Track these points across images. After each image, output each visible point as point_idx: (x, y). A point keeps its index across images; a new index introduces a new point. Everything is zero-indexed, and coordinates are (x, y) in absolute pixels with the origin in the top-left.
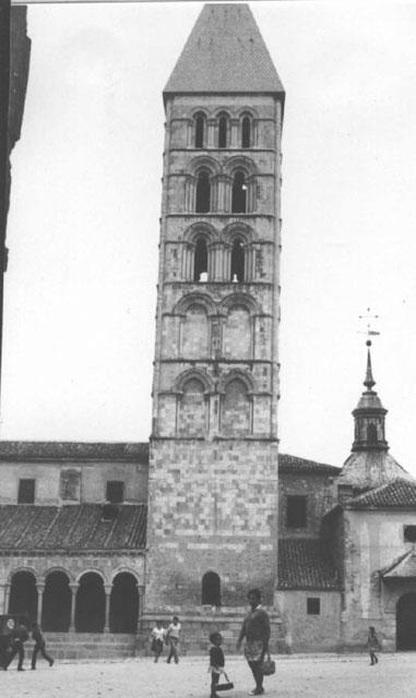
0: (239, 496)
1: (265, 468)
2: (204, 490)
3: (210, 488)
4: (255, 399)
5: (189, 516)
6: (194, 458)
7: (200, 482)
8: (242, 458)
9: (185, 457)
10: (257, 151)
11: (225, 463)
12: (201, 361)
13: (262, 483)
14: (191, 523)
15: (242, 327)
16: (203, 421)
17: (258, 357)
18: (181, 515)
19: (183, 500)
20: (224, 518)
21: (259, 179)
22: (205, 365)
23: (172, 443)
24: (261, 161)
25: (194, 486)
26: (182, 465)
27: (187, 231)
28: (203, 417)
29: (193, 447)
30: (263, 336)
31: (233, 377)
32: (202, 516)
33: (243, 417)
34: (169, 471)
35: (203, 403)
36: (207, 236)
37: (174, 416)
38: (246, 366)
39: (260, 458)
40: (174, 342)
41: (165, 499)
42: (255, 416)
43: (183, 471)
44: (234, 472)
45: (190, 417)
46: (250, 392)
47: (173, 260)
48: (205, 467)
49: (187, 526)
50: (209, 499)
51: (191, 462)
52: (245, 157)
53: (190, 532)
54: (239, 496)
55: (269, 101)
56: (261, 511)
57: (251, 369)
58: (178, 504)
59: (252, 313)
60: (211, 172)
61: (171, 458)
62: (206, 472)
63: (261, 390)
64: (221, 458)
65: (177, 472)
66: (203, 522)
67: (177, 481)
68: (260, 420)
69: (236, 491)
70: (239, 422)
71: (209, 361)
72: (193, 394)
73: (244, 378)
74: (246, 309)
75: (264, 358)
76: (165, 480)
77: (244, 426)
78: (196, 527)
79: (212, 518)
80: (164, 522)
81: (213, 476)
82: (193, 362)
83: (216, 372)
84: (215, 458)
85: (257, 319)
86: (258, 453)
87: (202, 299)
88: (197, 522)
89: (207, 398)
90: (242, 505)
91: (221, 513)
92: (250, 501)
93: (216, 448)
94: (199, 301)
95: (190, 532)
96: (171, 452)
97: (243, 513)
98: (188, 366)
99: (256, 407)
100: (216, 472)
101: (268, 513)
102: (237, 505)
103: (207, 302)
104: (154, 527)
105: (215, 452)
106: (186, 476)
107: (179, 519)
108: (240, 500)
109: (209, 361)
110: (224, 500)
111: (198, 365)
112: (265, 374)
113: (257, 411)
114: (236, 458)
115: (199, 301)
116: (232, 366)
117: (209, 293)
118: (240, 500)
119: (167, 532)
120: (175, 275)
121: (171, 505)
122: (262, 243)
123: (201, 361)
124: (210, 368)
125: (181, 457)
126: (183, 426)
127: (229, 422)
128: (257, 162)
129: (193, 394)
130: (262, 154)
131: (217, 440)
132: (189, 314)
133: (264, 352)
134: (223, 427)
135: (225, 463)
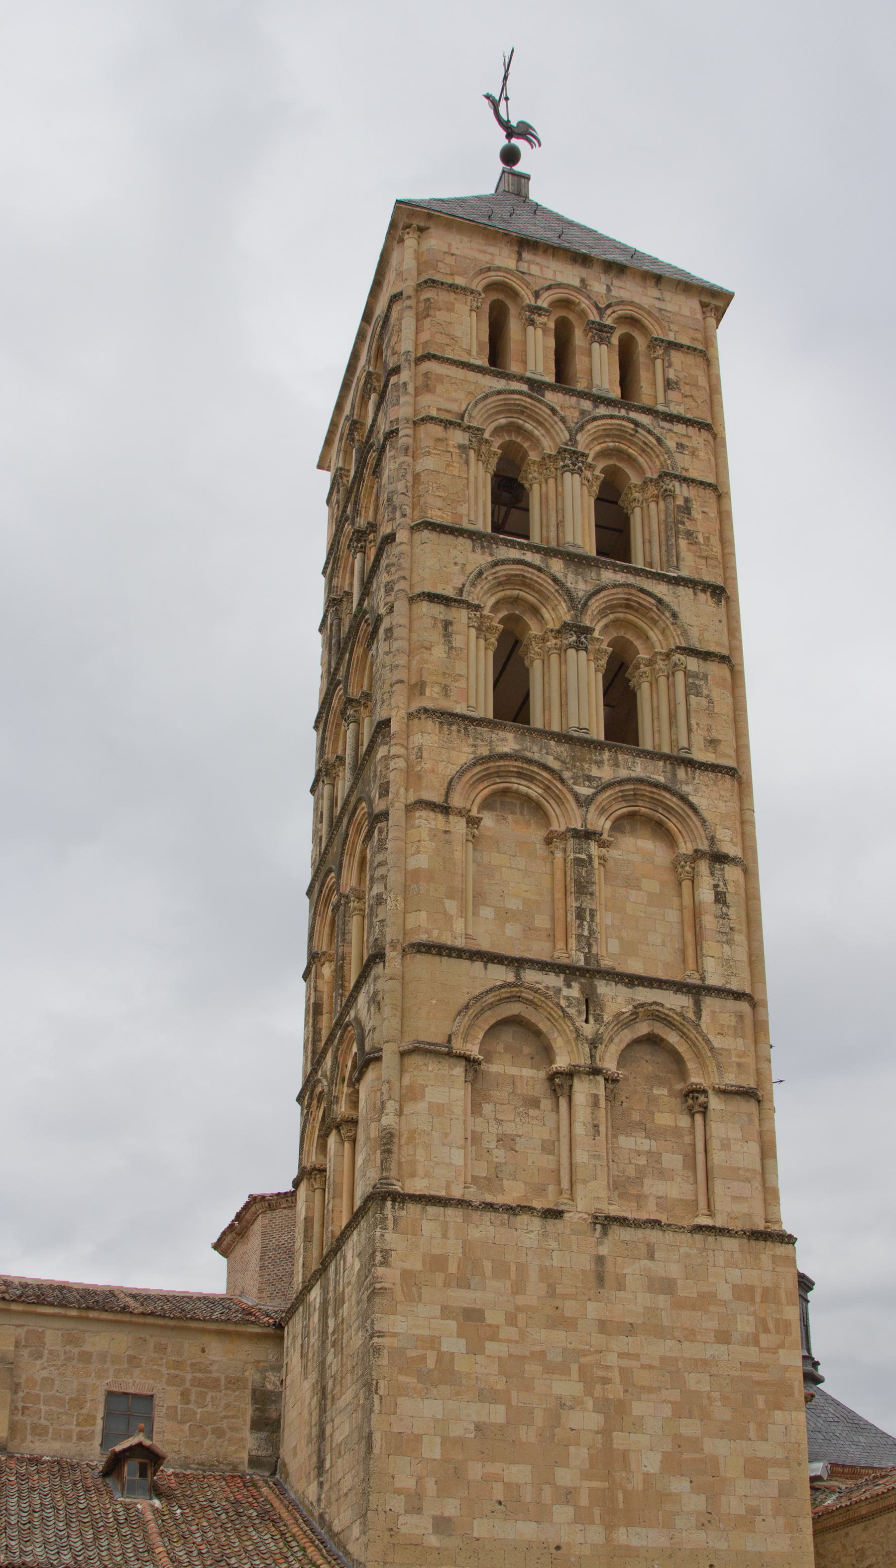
0: (677, 1414)
1: (762, 1325)
2: (567, 1387)
3: (584, 1375)
4: (715, 1103)
5: (519, 1473)
6: (533, 1274)
7: (555, 1357)
8: (687, 1289)
9: (501, 1270)
11: (633, 1301)
12: (543, 966)
13: (757, 1376)
14: (528, 1496)
15: (652, 886)
16: (547, 1161)
17: (713, 980)
18: (493, 1468)
19: (497, 1414)
20: (637, 1483)
21: (682, 491)
22: (553, 980)
23: (454, 1215)
24: (680, 446)
25: (533, 1369)
26: (490, 1296)
27: (480, 573)
28: (549, 1148)
29: (529, 1229)
30: (724, 916)
31: (643, 1028)
32: (565, 1477)
33: (673, 1161)
34: (446, 1312)
35: (546, 1103)
36: (535, 611)
37: (457, 1133)
39: (744, 1293)
40: (451, 896)
41: (432, 1408)
42: (718, 1157)
43: (494, 1317)
44: (660, 1332)
45: (506, 1141)
46: (695, 1079)
47: (439, 652)
48: (570, 1308)
49: (510, 1505)
50: (587, 1420)
51: (519, 1289)
52: (636, 424)
53: (527, 1530)
54: (681, 1411)
55: (686, 307)
56: (755, 1469)
57: (698, 1013)
58: (478, 1427)
59: (686, 847)
60: (536, 443)
61: (453, 1268)
62: (570, 1324)
63: (731, 1079)
64: (621, 1286)
65: (472, 1316)
66: (568, 1496)
67: (475, 1349)
68: (734, 1173)
69: (675, 1395)
70: (663, 1174)
71: (569, 971)
72: (513, 1071)
73: (672, 1038)
74: (660, 830)
75: (734, 985)
76: (433, 1342)
77: (676, 1189)
78: (542, 1515)
79: (595, 1484)
80: (430, 1486)
81: (597, 1340)
82: (518, 964)
83: (590, 1001)
84: (601, 1279)
85: (703, 867)
86: (735, 1275)
87: (531, 779)
88: (547, 1493)
89: (560, 1084)
90: (695, 1443)
91: (626, 1465)
92: (722, 1433)
93: (604, 1250)
94: (523, 787)
95: (527, 1530)
96: (453, 1248)
97: (709, 1478)
98: (500, 974)
99: (718, 1129)
100: (603, 1326)
101: (778, 1475)
102: (679, 1442)
103: (547, 788)
104: (398, 1503)
105: (600, 1260)
106: (510, 1332)
107: (487, 1479)
108: (690, 1428)
109: (569, 971)
110: (638, 1426)
111: (530, 976)
112: (738, 1032)
113: (725, 1145)
114: (667, 1286)
115: (523, 787)
116: (644, 995)
118: (690, 1428)
119: (442, 1525)
120: (446, 690)
121: (456, 1431)
122: (706, 656)
123: (543, 966)
124: (575, 991)
125: (488, 1266)
126: (482, 1171)
127: (631, 1171)
128: (671, 444)
129: (513, 1071)
130: (680, 428)
131: (605, 1222)
132: (488, 820)
133: (727, 963)
134: (620, 1187)
135: (633, 1301)
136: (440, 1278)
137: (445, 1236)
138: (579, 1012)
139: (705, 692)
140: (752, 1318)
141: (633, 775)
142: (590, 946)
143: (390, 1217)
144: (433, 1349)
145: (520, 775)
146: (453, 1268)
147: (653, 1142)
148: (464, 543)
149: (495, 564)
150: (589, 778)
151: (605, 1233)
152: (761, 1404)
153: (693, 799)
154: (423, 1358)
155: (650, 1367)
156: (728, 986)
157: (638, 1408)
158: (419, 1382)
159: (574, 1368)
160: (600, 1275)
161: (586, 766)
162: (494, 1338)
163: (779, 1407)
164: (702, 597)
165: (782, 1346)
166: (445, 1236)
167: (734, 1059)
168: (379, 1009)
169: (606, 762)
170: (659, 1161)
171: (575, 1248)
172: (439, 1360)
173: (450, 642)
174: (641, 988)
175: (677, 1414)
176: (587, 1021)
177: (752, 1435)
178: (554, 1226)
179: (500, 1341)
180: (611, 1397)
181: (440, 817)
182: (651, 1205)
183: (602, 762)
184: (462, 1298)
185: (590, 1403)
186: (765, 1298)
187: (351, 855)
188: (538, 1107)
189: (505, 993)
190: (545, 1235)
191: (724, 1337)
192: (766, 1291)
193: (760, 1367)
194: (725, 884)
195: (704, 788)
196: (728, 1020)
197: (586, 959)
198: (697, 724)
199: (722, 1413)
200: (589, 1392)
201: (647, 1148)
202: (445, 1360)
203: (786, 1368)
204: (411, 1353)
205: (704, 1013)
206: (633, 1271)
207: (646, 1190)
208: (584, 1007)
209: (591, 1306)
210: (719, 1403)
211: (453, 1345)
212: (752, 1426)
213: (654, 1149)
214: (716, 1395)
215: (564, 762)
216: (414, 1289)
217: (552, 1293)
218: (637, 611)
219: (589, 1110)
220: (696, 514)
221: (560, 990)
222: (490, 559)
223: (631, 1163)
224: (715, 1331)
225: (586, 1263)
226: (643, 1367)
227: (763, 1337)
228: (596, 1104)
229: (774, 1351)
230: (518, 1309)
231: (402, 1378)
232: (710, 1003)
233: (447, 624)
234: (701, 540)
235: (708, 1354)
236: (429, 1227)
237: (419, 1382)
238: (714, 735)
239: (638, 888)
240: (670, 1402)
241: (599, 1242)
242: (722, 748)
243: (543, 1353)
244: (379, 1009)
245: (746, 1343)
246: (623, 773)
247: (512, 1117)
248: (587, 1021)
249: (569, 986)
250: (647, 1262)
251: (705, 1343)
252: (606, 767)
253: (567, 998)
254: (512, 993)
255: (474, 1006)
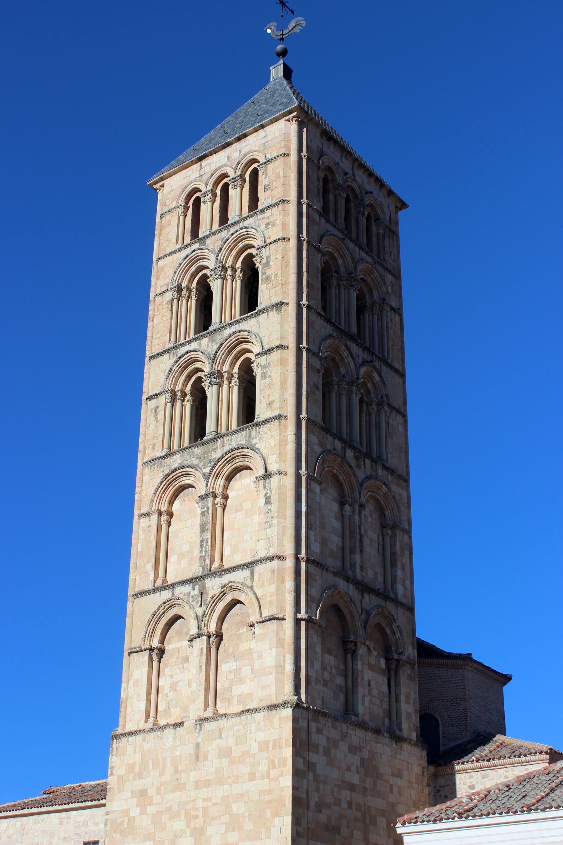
2: (179, 825)
10: (266, 209)
13: (267, 798)
30: (269, 511)
38: (246, 573)
39: (264, 746)
43: (152, 792)
51: (162, 774)
57: (252, 579)
61: (137, 770)
64: (206, 759)
65: (143, 793)
67: (143, 812)
76: (126, 813)
84: (197, 757)
93: (199, 740)
100: (198, 785)
105: (198, 745)
113: (260, 656)
114: (225, 753)
117: (195, 461)
125: (151, 763)
130: (268, 213)
135: (211, 765)
136: (132, 775)
137: (135, 752)
138: (197, 602)
139: (269, 374)
140: (267, 761)
141: (230, 447)
142: (205, 561)
143: (115, 748)
144: (127, 816)
146: (137, 770)
147: (238, 663)
148: (166, 356)
149: (177, 361)
150: (210, 461)
151: (201, 729)
152: (268, 815)
153: (257, 446)
154: (123, 822)
155: (216, 804)
156: (268, 555)
157: (210, 830)
158: (121, 836)
159: (183, 812)
160: (198, 755)
161: (209, 455)
162: (151, 804)
163: (277, 815)
164: (271, 313)
165: (281, 775)
166: (135, 752)
167: (269, 599)
169: (219, 447)
173: (157, 418)
174: (226, 575)
175: (227, 831)
176: (201, 605)
177: (263, 837)
178: (180, 730)
179: (153, 805)
180: (198, 826)
181: (147, 519)
182: (235, 701)
183: (217, 448)
184: (139, 784)
185: (188, 832)
186: (274, 748)
189: (167, 605)
190: (174, 739)
191: (252, 777)
192: (275, 741)
193: (270, 792)
194: (271, 491)
195: (264, 435)
196: (268, 575)
197: (203, 569)
198: (263, 397)
199: (249, 826)
200: (188, 826)
201: (234, 667)
202: (131, 820)
203: (283, 789)
204: (119, 821)
205: (255, 577)
206: (211, 748)
207: (234, 693)
208: (200, 599)
209: (192, 773)
210: (247, 819)
211: (135, 812)
212: (263, 830)
214: (246, 814)
215: (200, 458)
216: (122, 785)
217: (176, 771)
219: (198, 658)
220: (271, 263)
221: (189, 593)
222: (175, 358)
223: (227, 679)
224: (249, 774)
225: (191, 749)
226: (213, 804)
227: (272, 772)
228: (202, 654)
229: (277, 779)
230: (162, 784)
231: (115, 835)
232: (258, 569)
233: (157, 407)
234: (273, 278)
235: (244, 790)
236: (130, 749)
237: (121, 836)
238: (272, 398)
239: (241, 510)
240: (224, 823)
241: (198, 736)
242: (277, 404)
243: (170, 807)
245: (263, 778)
246: (227, 448)
248: (201, 605)
249: (194, 589)
250: (218, 740)
251: (243, 783)
252: (219, 450)
253: (193, 597)
254: (169, 604)
255: (156, 617)
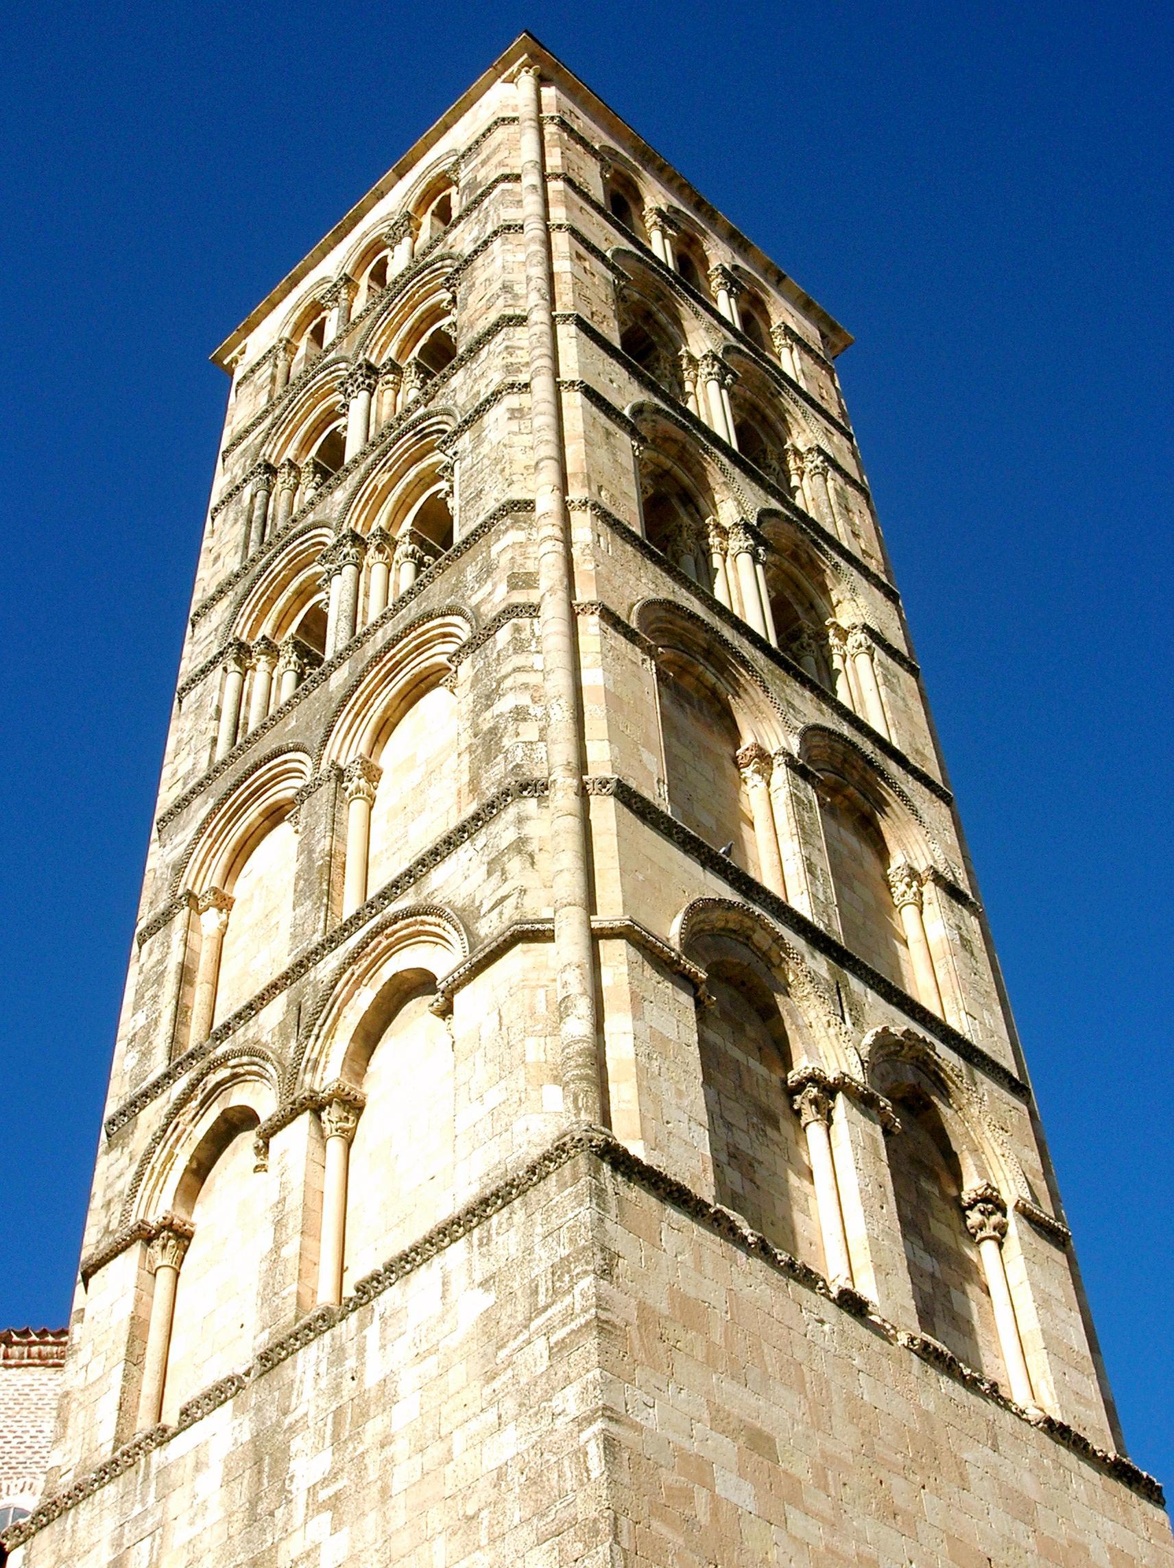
34: (719, 1419)
65: (759, 1443)
143: (610, 1191)
145: (708, 654)
161: (788, 691)
168: (533, 864)
170: (947, 1296)
171: (889, 1380)
172: (715, 1513)
187: (357, 715)
188: (778, 1129)
213: (938, 1274)
218: (802, 567)
244: (533, 864)
247: (744, 1125)
